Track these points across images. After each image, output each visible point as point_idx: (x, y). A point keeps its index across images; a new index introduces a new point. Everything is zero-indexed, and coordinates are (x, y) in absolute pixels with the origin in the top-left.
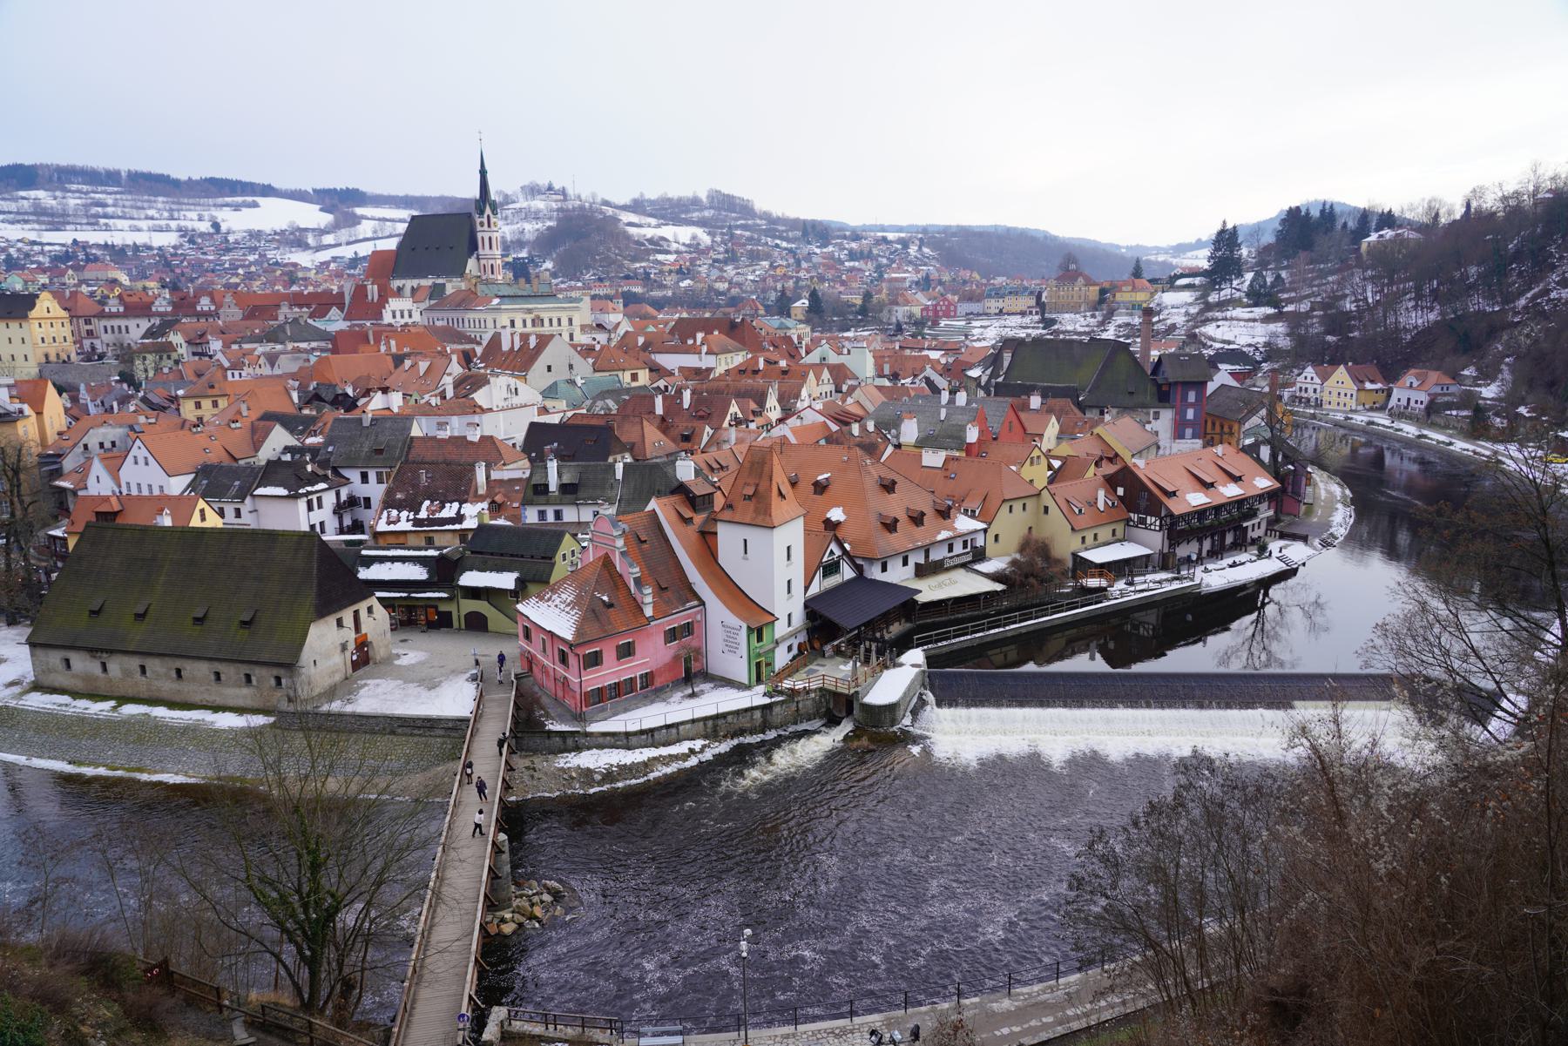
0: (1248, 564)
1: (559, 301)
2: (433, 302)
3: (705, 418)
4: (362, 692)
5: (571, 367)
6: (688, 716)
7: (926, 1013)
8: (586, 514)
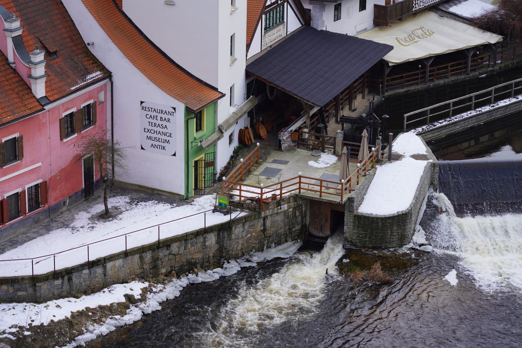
6: (118, 247)
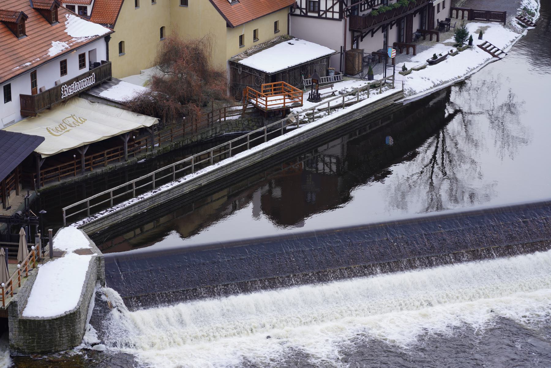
0: (450, 58)
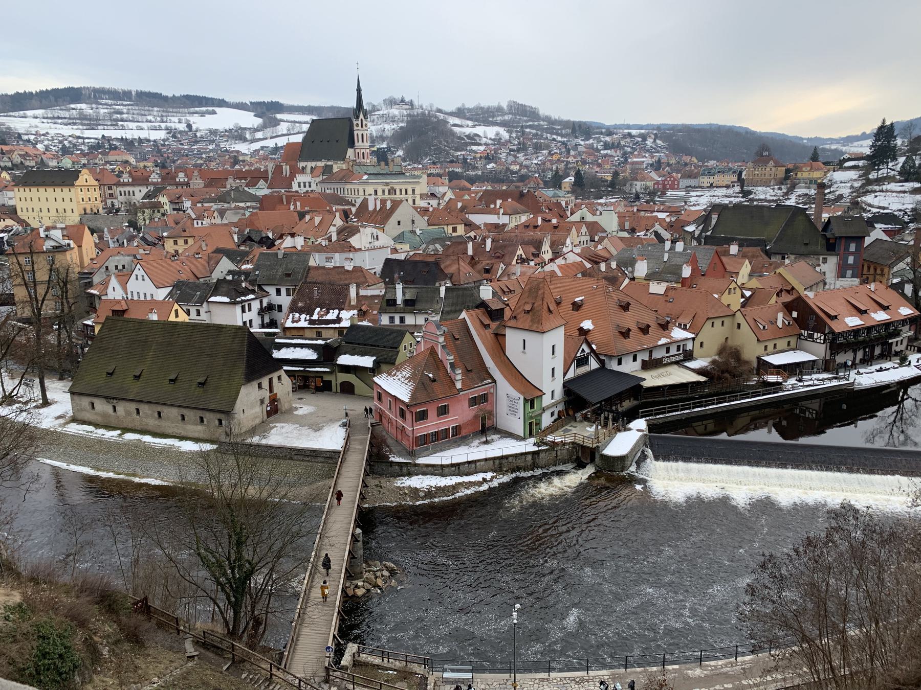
1: (407, 178)
2: (324, 177)
3: (500, 257)
4: (273, 431)
5: (413, 222)
6: (482, 456)
7: (640, 673)
8: (420, 320)
